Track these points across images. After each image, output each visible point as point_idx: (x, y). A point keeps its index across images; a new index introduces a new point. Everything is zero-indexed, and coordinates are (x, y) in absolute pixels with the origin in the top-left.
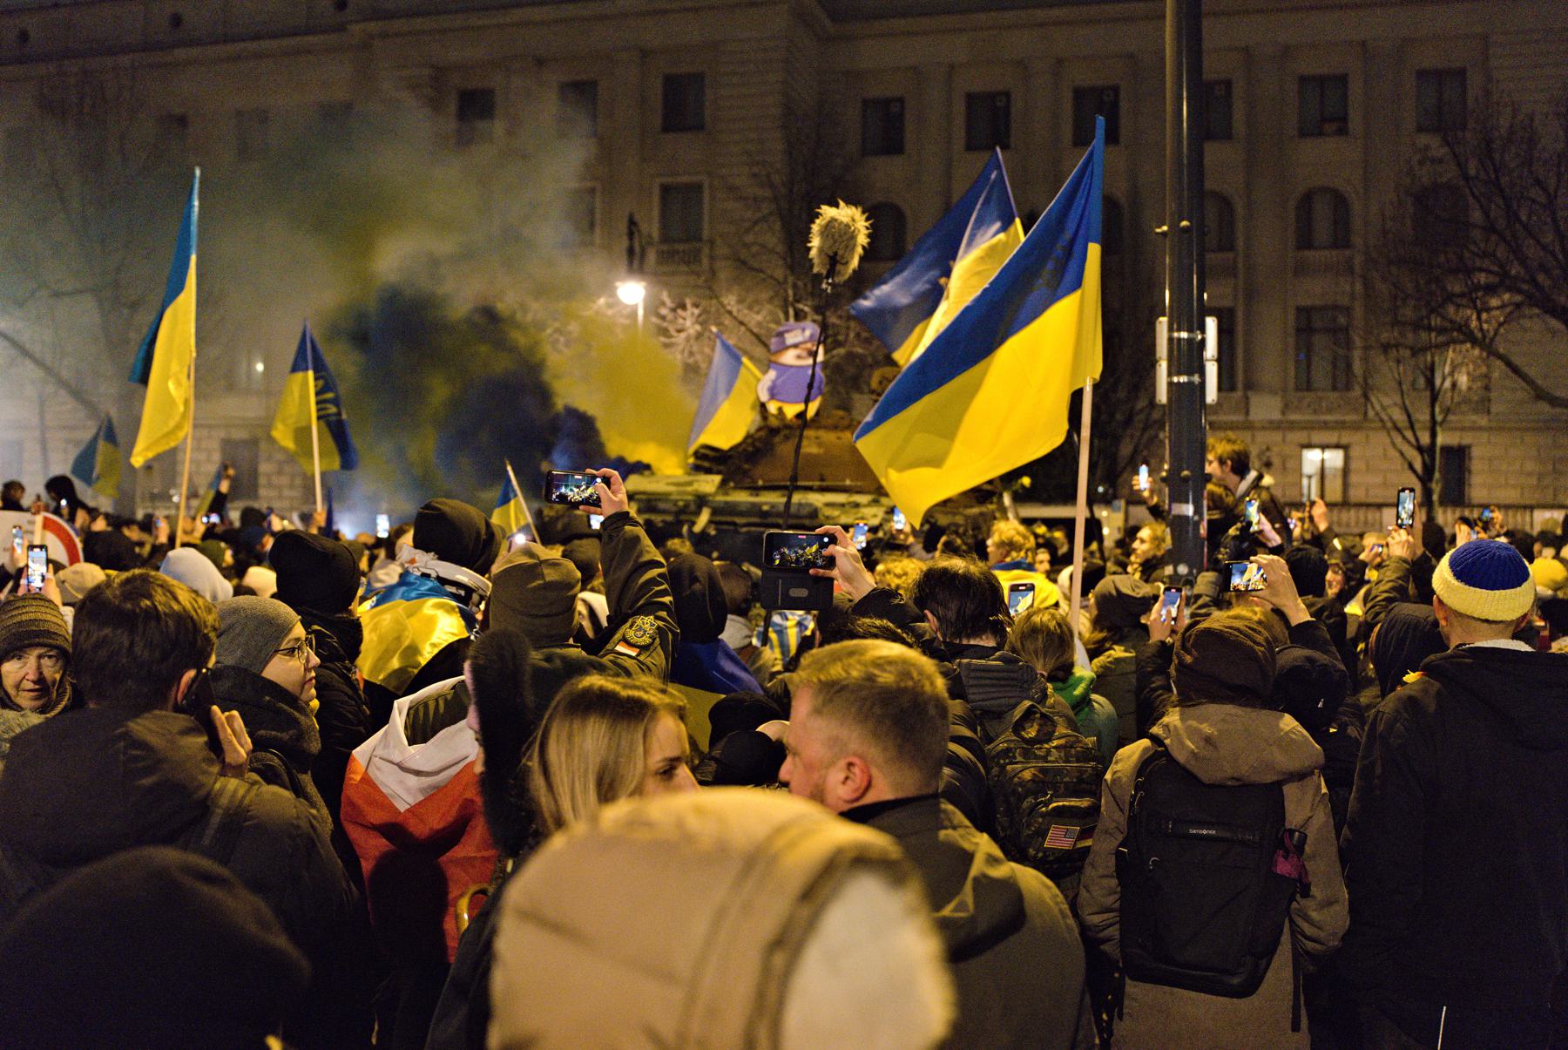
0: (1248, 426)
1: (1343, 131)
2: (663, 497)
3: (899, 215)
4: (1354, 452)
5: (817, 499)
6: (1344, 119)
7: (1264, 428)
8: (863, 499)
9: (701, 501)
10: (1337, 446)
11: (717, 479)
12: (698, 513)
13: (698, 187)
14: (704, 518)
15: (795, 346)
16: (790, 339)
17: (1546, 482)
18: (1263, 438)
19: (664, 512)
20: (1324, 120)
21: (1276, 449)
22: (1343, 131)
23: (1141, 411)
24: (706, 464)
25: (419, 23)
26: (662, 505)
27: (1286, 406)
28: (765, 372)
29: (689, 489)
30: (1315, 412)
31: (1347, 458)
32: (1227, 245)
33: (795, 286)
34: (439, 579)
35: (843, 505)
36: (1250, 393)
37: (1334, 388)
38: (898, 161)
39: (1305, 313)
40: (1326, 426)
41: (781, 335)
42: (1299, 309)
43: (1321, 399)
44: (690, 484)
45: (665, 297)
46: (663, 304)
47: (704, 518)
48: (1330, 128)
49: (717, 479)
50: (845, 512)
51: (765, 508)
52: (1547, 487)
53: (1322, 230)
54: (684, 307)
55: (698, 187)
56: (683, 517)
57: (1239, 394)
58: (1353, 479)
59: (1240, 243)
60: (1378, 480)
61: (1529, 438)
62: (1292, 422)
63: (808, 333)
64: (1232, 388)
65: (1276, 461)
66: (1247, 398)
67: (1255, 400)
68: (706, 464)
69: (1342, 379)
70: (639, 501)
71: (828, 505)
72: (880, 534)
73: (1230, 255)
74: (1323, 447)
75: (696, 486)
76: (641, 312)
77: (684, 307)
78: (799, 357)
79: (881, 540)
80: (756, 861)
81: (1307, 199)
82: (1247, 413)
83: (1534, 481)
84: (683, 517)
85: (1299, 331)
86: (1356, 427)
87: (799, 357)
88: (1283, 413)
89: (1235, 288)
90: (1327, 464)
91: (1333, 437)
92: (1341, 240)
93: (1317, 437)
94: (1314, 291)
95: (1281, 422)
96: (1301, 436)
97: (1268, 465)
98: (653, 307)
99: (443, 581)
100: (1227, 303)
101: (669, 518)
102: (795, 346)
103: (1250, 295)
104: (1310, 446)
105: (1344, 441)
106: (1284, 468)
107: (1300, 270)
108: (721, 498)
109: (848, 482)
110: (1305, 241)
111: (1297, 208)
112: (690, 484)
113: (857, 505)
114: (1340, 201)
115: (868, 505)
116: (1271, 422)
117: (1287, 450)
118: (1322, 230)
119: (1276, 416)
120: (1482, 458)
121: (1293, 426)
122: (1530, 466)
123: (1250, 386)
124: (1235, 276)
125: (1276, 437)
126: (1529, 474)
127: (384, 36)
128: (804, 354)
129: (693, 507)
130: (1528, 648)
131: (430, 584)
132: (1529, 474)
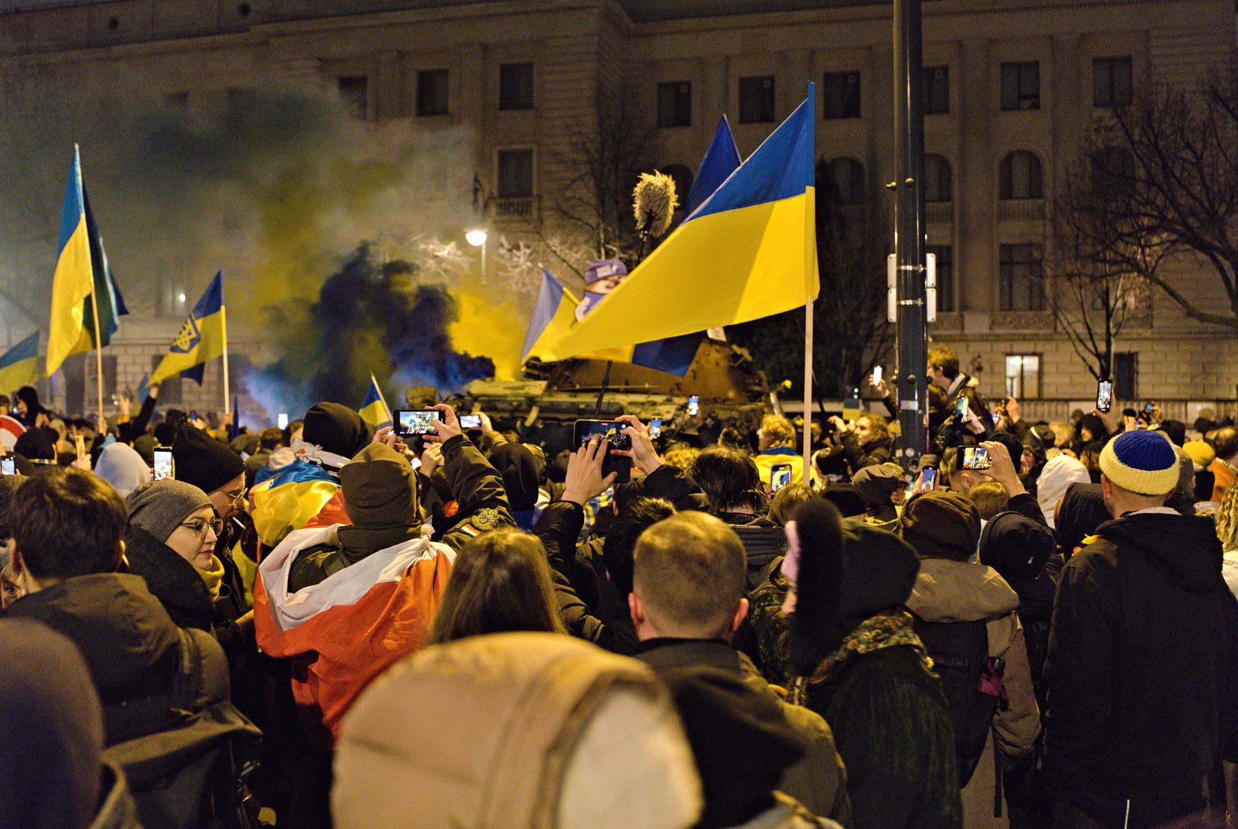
0: (965, 339)
1: (1036, 106)
2: (502, 398)
4: (1046, 359)
5: (622, 399)
6: (1037, 97)
7: (976, 341)
8: (659, 399)
9: (531, 401)
10: (1033, 354)
11: (544, 384)
12: (529, 411)
13: (528, 153)
14: (533, 415)
15: (605, 278)
16: (601, 272)
17: (1198, 380)
18: (975, 348)
19: (503, 410)
20: (1022, 97)
21: (985, 357)
22: (1036, 106)
24: (536, 372)
25: (305, 25)
26: (500, 405)
27: (993, 322)
28: (581, 299)
29: (522, 392)
30: (1016, 328)
31: (1041, 364)
33: (606, 231)
34: (323, 465)
35: (643, 404)
37: (1031, 309)
38: (687, 131)
39: (1006, 248)
40: (1024, 338)
41: (593, 269)
42: (1003, 246)
43: (1020, 317)
44: (522, 388)
45: (503, 240)
46: (502, 245)
47: (533, 415)
48: (1026, 103)
49: (544, 384)
50: (646, 410)
51: (582, 406)
52: (1196, 385)
53: (1020, 185)
54: (518, 248)
55: (528, 153)
56: (517, 414)
57: (955, 314)
58: (1046, 379)
60: (1067, 380)
61: (1183, 346)
62: (998, 335)
63: (615, 268)
64: (951, 309)
65: (986, 367)
66: (962, 316)
67: (969, 319)
68: (536, 372)
69: (1037, 301)
70: (481, 402)
71: (631, 404)
72: (673, 426)
73: (948, 204)
74: (1023, 355)
75: (527, 390)
76: (484, 252)
77: (518, 248)
78: (608, 287)
79: (673, 431)
80: (538, 686)
81: (1007, 162)
82: (963, 329)
83: (1188, 380)
84: (517, 414)
85: (1002, 263)
86: (1048, 339)
87: (608, 287)
88: (991, 328)
89: (953, 228)
90: (1026, 368)
91: (1030, 347)
92: (1035, 191)
93: (1017, 347)
94: (1015, 231)
95: (988, 335)
96: (1005, 346)
97: (979, 369)
98: (492, 245)
99: (326, 467)
100: (947, 242)
101: (506, 415)
102: (605, 278)
103: (965, 235)
104: (1012, 354)
105: (1039, 350)
107: (1004, 215)
108: (546, 399)
109: (647, 386)
110: (1007, 192)
112: (522, 388)
113: (654, 404)
114: (1034, 162)
115: (663, 404)
116: (981, 336)
118: (1020, 185)
119: (986, 330)
121: (998, 338)
123: (965, 307)
125: (984, 347)
126: (1185, 374)
127: (280, 35)
128: (612, 284)
129: (525, 407)
130: (1176, 513)
131: (316, 470)
132: (1185, 374)
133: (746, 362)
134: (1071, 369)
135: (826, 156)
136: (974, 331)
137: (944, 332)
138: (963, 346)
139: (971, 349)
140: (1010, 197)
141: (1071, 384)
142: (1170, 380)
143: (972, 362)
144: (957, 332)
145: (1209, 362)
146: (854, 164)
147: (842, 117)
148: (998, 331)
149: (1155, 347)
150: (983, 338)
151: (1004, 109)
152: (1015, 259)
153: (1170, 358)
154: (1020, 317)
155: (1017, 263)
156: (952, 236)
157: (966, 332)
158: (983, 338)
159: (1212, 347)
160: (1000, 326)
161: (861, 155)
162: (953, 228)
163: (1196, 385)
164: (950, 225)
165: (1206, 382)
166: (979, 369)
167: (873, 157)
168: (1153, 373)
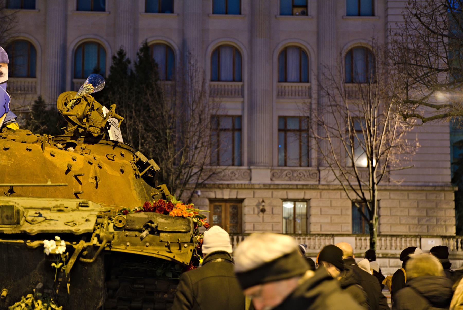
0: (251, 187)
1: (305, 13)
3: (31, 48)
4: (313, 203)
6: (306, 6)
7: (260, 189)
10: (303, 200)
17: (423, 222)
18: (261, 194)
20: (294, 6)
21: (267, 202)
22: (305, 13)
23: (195, 173)
27: (273, 175)
30: (290, 179)
31: (308, 208)
32: (238, 78)
36: (252, 167)
37: (301, 166)
38: (31, 13)
39: (283, 119)
40: (297, 188)
42: (280, 117)
43: (293, 171)
48: (297, 11)
52: (422, 225)
53: (293, 71)
57: (245, 167)
58: (313, 219)
59: (246, 77)
60: (328, 220)
61: (412, 196)
62: (278, 185)
64: (241, 164)
65: (268, 209)
66: (250, 170)
69: (305, 158)
72: (95, 241)
73: (240, 84)
74: (295, 201)
79: (95, 247)
81: (284, 53)
82: (250, 180)
83: (416, 221)
85: (279, 130)
88: (271, 180)
89: (243, 102)
90: (297, 211)
91: (299, 194)
92: (304, 78)
93: (293, 194)
94: (293, 108)
95: (270, 185)
96: (282, 194)
97: (263, 211)
100: (239, 113)
103: (252, 107)
104: (286, 200)
105: (307, 197)
106: (272, 213)
107: (281, 94)
110: (284, 78)
111: (279, 58)
114: (303, 54)
116: (264, 185)
117: (275, 202)
118: (293, 71)
119: (269, 182)
120: (386, 207)
121: (278, 187)
122: (413, 212)
123: (251, 163)
124: (243, 96)
125: (267, 194)
126: (414, 217)
132: (414, 217)
133: (152, 171)
134: (331, 212)
135: (149, 41)
136: (258, 182)
137: (236, 182)
138: (251, 192)
139: (256, 195)
140: (286, 81)
141: (331, 223)
142: (403, 222)
143: (257, 206)
144: (247, 182)
145: (431, 209)
146: (169, 49)
147: (160, 12)
148: (277, 182)
149: (392, 196)
150: (267, 187)
151: (281, 14)
152: (288, 128)
153: (404, 204)
154: (293, 171)
155: (290, 130)
156: (243, 110)
157: (253, 182)
158: (267, 187)
159: (432, 197)
160: (279, 178)
161: (175, 43)
162: (243, 102)
163: (422, 225)
164: (241, 99)
165: (428, 223)
166: (263, 211)
167: (184, 43)
168: (391, 215)
